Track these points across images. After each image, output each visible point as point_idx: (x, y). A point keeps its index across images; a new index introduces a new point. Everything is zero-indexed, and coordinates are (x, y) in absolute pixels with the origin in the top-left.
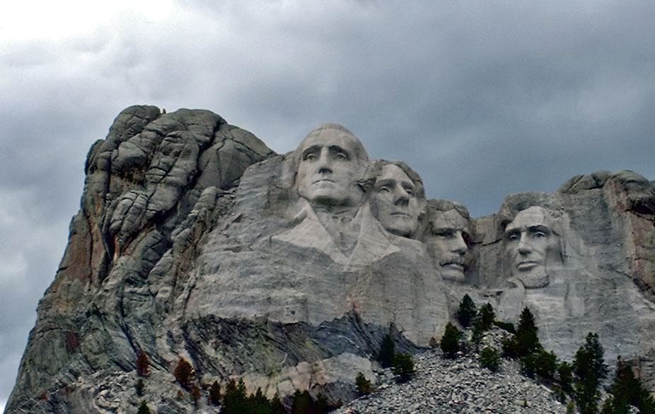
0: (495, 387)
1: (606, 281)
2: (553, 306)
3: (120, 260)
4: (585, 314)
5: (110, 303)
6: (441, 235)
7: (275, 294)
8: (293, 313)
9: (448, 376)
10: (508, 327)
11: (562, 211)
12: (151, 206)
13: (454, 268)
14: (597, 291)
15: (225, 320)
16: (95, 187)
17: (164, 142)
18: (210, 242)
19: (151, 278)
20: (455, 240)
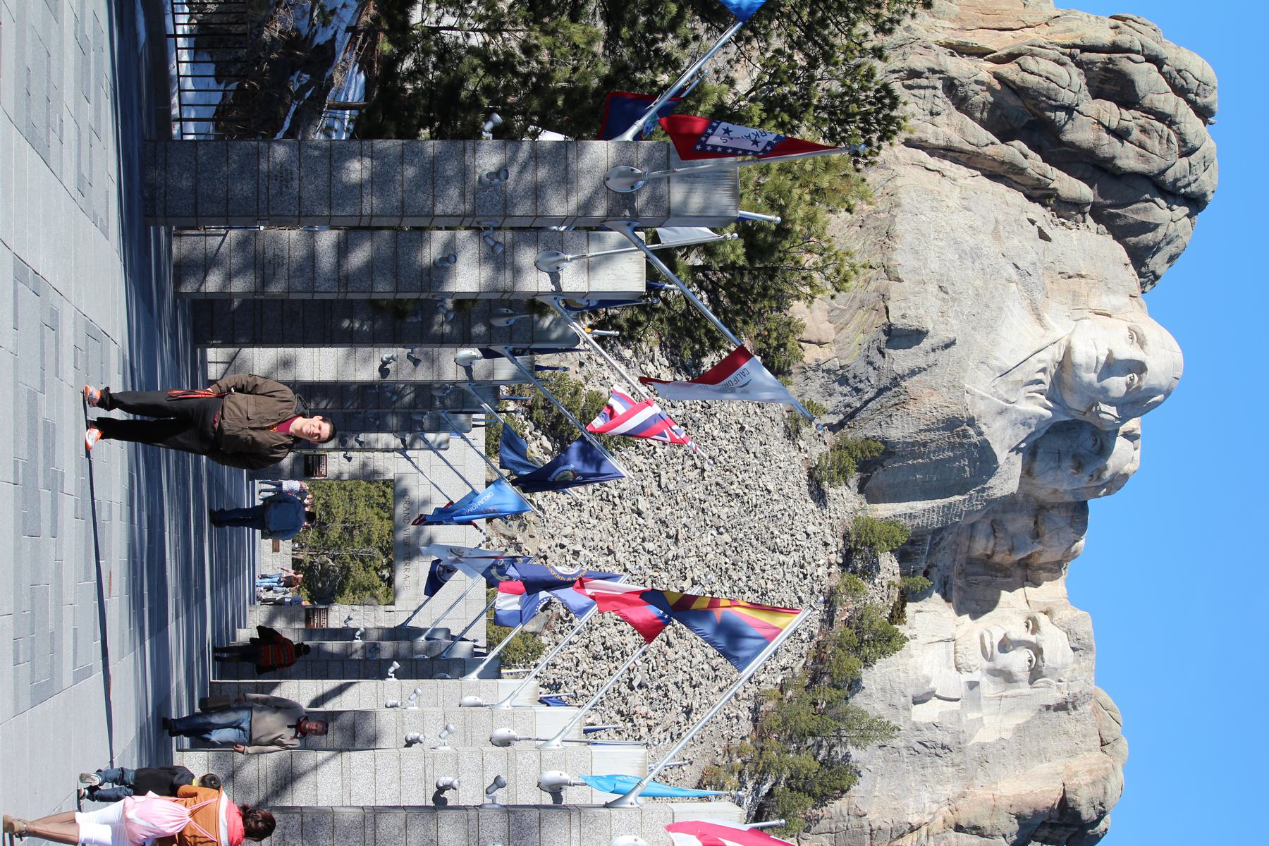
0: (800, 594)
3: (984, 70)
4: (914, 723)
6: (1036, 523)
8: (904, 316)
9: (816, 529)
11: (1066, 692)
13: (988, 541)
14: (947, 740)
15: (892, 222)
19: (958, 117)
20: (1029, 540)
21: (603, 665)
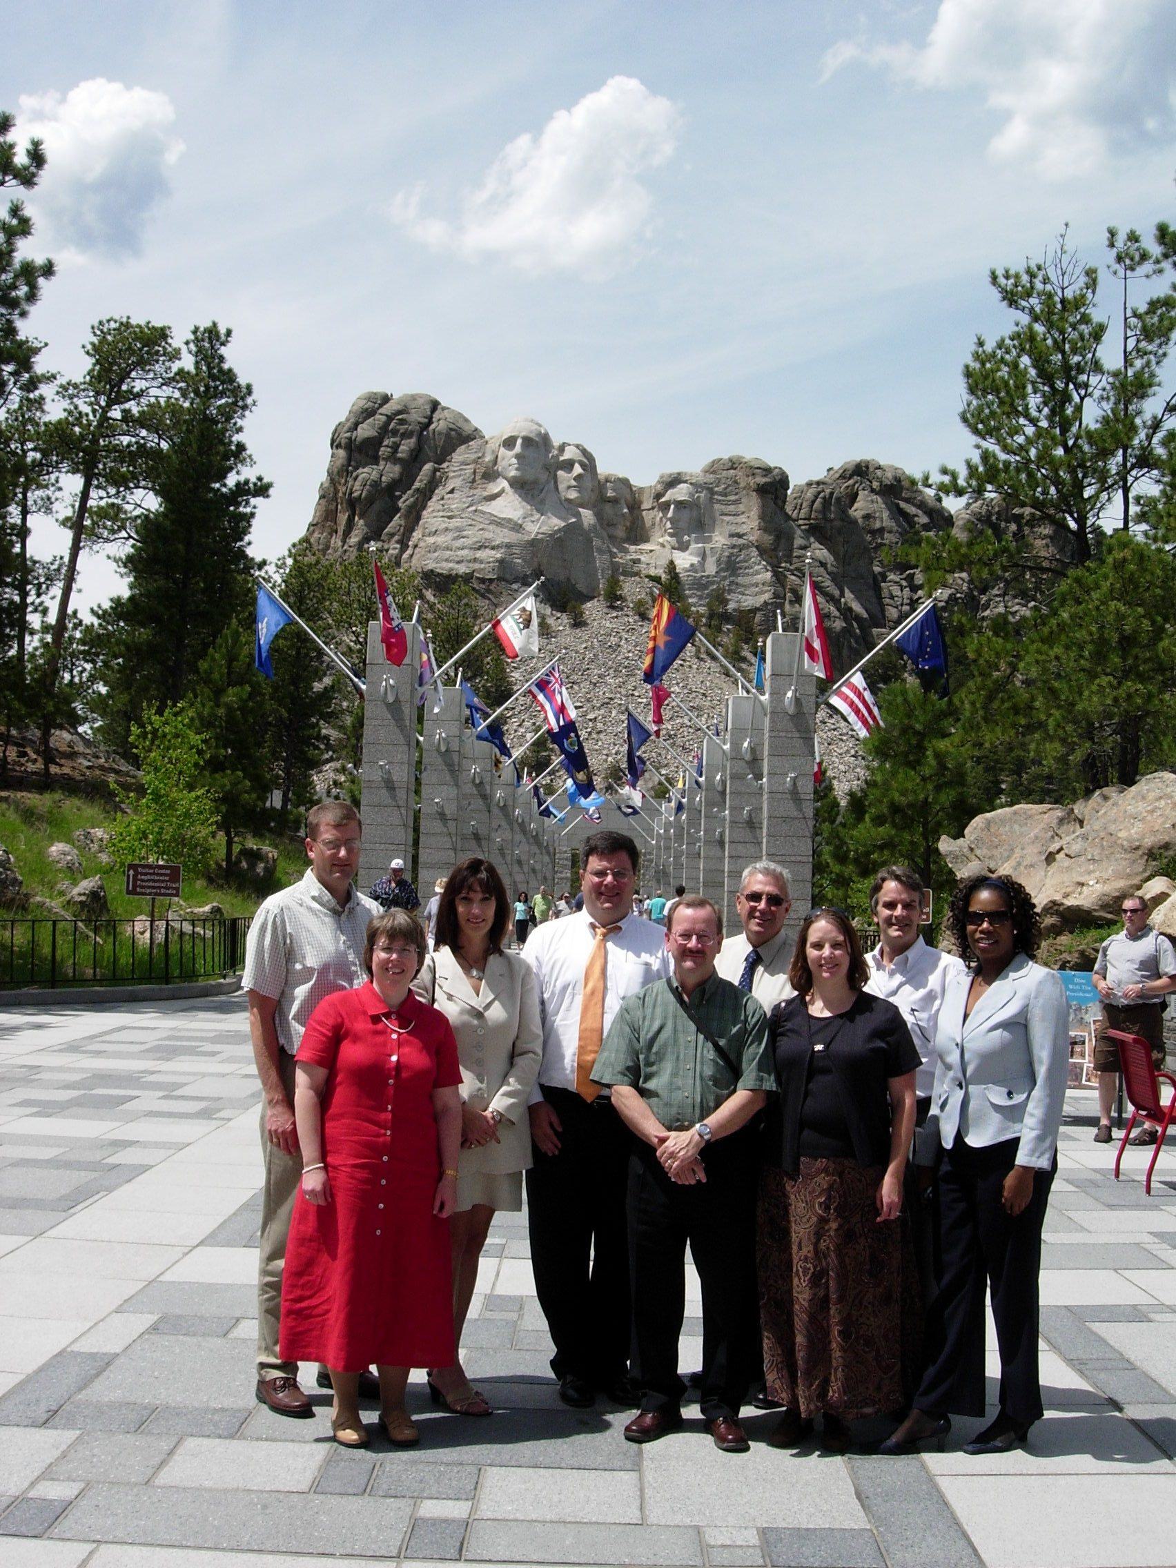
1: (734, 547)
2: (692, 565)
3: (360, 522)
5: (353, 555)
7: (479, 554)
10: (656, 579)
12: (384, 479)
14: (726, 554)
16: (339, 463)
17: (392, 425)
18: (430, 510)
21: (679, 741)
